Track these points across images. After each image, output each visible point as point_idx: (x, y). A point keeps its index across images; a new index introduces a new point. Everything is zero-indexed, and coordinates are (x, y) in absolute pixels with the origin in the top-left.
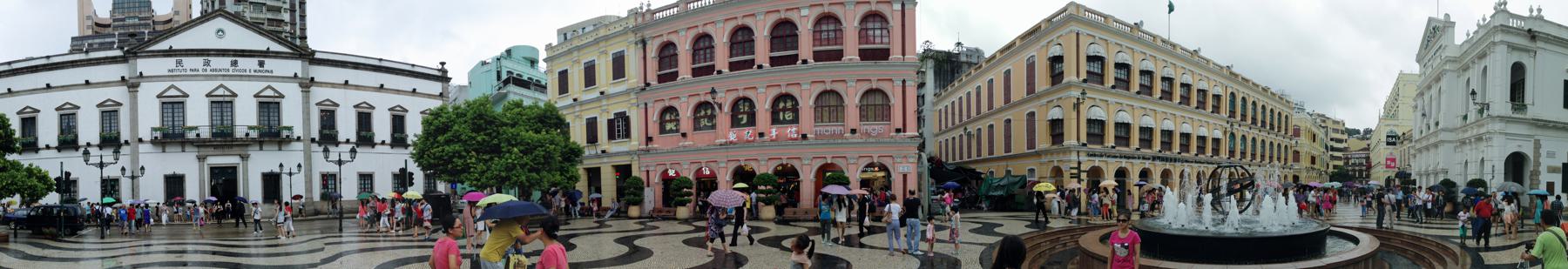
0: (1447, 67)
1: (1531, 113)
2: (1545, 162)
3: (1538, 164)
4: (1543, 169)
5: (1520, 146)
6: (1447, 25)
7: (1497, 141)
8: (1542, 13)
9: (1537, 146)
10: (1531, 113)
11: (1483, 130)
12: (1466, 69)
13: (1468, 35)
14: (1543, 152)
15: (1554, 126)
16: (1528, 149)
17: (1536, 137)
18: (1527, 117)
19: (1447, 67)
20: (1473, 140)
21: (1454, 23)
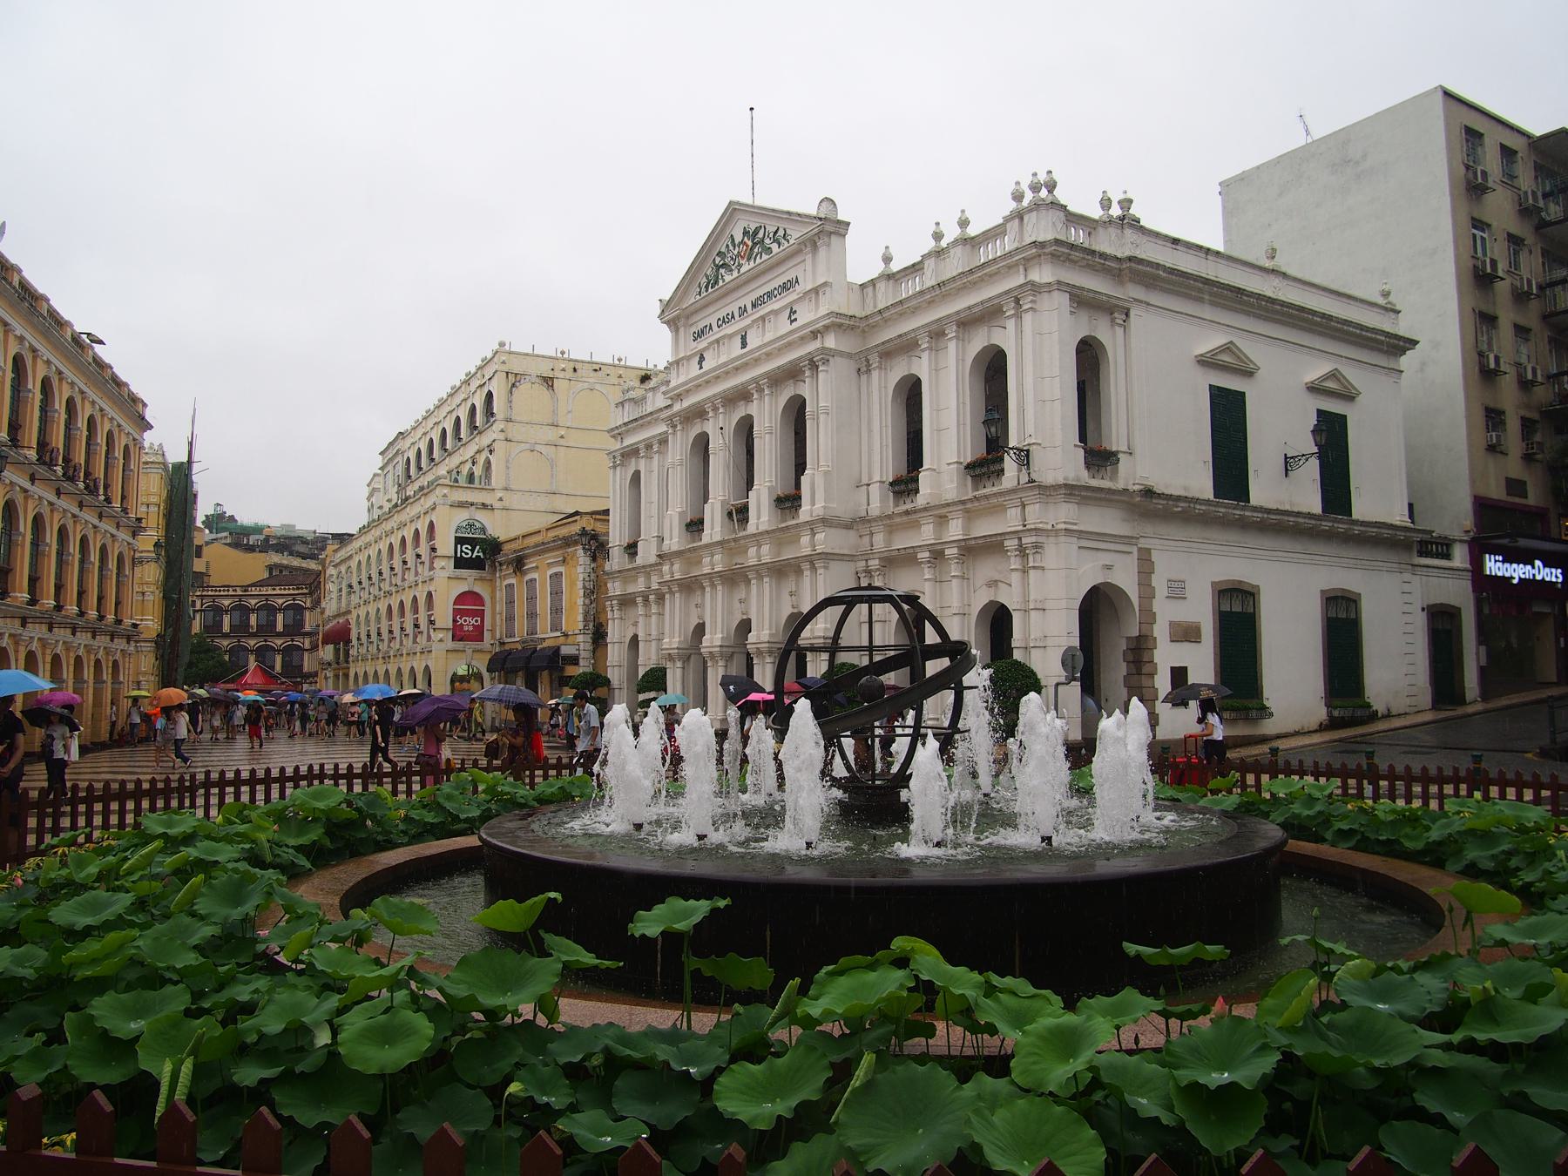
0: (831, 342)
1: (1130, 474)
2: (1166, 613)
3: (1149, 617)
4: (1160, 631)
5: (1109, 567)
6: (829, 228)
7: (1057, 554)
8: (1134, 211)
9: (1146, 567)
10: (1130, 474)
11: (986, 528)
12: (907, 346)
13: (887, 259)
14: (1159, 582)
15: (1184, 511)
16: (1125, 578)
17: (1143, 543)
18: (1120, 485)
19: (831, 342)
20: (951, 552)
21: (848, 224)
